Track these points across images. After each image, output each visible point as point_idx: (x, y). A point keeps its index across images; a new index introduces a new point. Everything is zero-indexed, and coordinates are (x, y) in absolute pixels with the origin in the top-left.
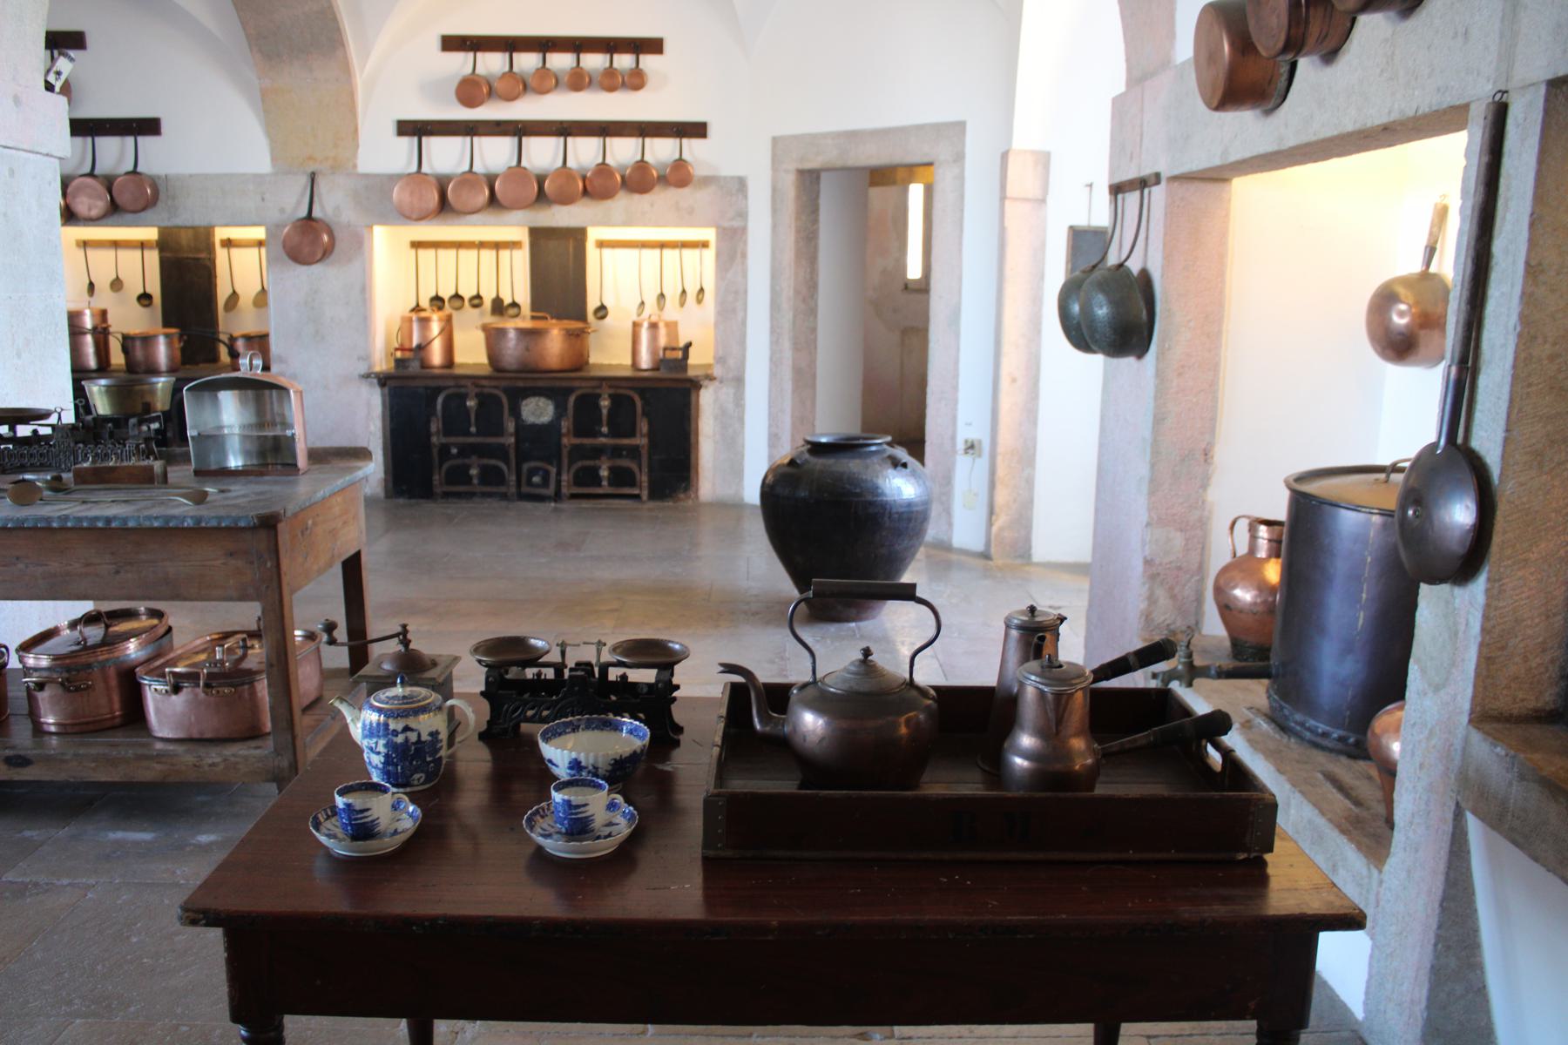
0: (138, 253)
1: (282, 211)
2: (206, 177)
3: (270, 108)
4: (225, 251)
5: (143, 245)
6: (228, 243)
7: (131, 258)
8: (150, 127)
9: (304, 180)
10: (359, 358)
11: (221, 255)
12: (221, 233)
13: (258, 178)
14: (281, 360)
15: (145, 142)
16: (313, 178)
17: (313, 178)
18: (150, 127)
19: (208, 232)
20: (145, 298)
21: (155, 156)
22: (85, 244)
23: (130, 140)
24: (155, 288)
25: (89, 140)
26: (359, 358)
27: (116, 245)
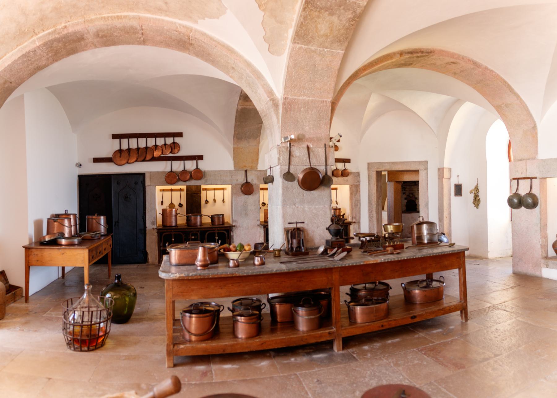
0: (179, 192)
1: (237, 180)
2: (216, 171)
3: (236, 155)
4: (205, 191)
5: (181, 190)
6: (206, 189)
7: (176, 194)
8: (201, 158)
9: (244, 173)
10: (258, 220)
11: (203, 193)
12: (203, 187)
13: (230, 172)
14: (236, 221)
15: (199, 162)
16: (246, 171)
17: (246, 171)
18: (201, 158)
19: (200, 186)
20: (181, 205)
21: (202, 165)
22: (163, 190)
23: (195, 161)
24: (184, 203)
25: (183, 162)
26: (258, 220)
27: (172, 190)
